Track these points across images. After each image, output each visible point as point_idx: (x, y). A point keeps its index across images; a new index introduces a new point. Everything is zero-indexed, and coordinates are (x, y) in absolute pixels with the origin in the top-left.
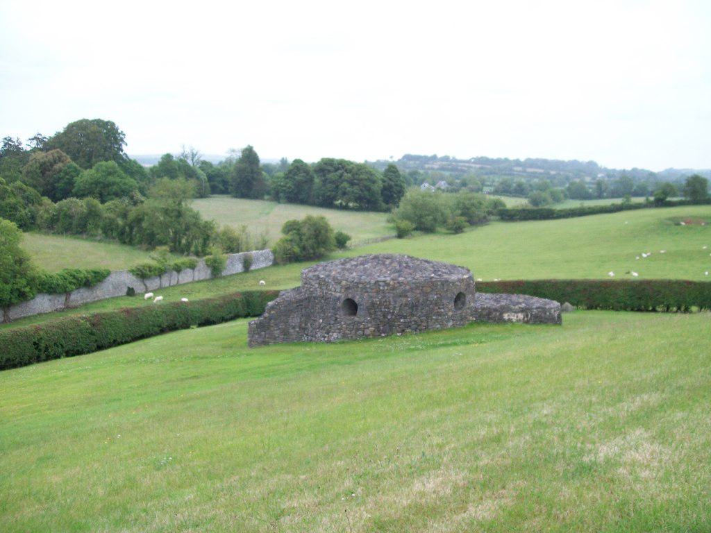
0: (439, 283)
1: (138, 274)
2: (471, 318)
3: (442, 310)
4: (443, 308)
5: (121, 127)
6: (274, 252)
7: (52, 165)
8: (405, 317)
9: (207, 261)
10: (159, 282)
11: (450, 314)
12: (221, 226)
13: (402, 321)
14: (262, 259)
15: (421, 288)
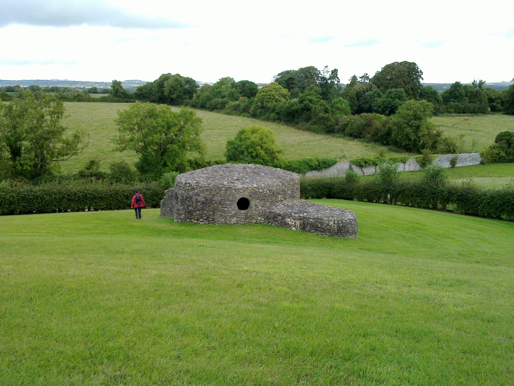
0: (224, 189)
1: (357, 165)
2: (259, 218)
3: (225, 209)
4: (226, 208)
5: (421, 66)
6: (482, 155)
7: (365, 93)
8: (199, 210)
9: (417, 158)
10: (374, 170)
11: (233, 212)
12: (445, 135)
13: (197, 212)
14: (468, 159)
15: (209, 191)
